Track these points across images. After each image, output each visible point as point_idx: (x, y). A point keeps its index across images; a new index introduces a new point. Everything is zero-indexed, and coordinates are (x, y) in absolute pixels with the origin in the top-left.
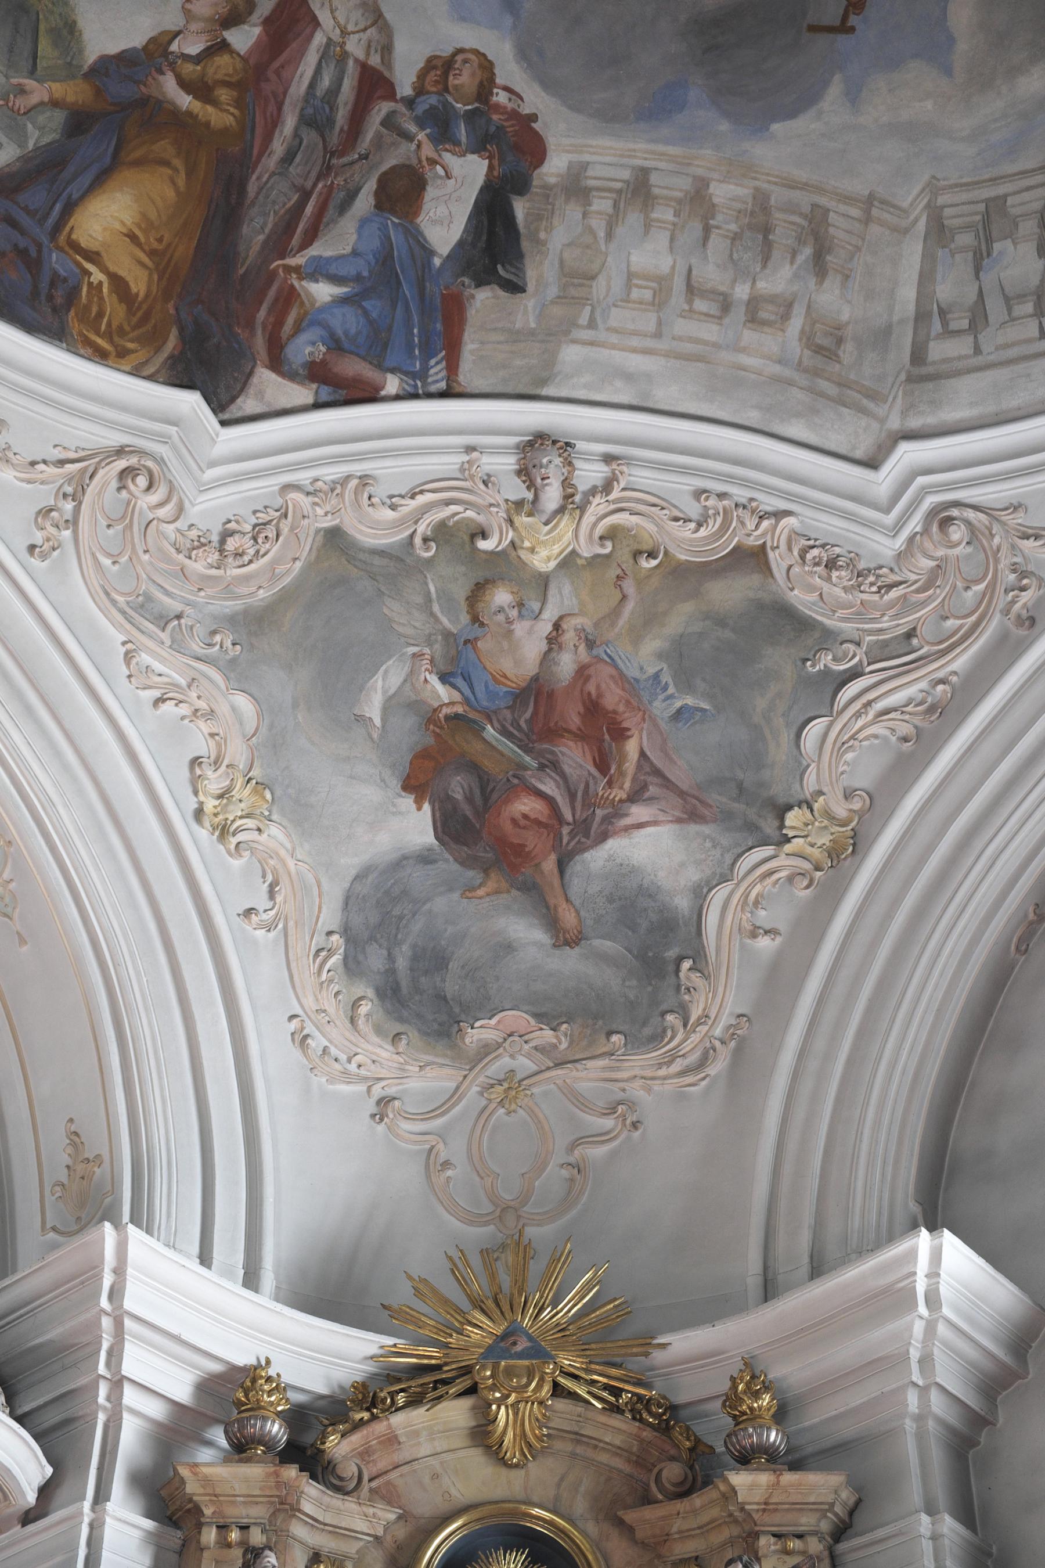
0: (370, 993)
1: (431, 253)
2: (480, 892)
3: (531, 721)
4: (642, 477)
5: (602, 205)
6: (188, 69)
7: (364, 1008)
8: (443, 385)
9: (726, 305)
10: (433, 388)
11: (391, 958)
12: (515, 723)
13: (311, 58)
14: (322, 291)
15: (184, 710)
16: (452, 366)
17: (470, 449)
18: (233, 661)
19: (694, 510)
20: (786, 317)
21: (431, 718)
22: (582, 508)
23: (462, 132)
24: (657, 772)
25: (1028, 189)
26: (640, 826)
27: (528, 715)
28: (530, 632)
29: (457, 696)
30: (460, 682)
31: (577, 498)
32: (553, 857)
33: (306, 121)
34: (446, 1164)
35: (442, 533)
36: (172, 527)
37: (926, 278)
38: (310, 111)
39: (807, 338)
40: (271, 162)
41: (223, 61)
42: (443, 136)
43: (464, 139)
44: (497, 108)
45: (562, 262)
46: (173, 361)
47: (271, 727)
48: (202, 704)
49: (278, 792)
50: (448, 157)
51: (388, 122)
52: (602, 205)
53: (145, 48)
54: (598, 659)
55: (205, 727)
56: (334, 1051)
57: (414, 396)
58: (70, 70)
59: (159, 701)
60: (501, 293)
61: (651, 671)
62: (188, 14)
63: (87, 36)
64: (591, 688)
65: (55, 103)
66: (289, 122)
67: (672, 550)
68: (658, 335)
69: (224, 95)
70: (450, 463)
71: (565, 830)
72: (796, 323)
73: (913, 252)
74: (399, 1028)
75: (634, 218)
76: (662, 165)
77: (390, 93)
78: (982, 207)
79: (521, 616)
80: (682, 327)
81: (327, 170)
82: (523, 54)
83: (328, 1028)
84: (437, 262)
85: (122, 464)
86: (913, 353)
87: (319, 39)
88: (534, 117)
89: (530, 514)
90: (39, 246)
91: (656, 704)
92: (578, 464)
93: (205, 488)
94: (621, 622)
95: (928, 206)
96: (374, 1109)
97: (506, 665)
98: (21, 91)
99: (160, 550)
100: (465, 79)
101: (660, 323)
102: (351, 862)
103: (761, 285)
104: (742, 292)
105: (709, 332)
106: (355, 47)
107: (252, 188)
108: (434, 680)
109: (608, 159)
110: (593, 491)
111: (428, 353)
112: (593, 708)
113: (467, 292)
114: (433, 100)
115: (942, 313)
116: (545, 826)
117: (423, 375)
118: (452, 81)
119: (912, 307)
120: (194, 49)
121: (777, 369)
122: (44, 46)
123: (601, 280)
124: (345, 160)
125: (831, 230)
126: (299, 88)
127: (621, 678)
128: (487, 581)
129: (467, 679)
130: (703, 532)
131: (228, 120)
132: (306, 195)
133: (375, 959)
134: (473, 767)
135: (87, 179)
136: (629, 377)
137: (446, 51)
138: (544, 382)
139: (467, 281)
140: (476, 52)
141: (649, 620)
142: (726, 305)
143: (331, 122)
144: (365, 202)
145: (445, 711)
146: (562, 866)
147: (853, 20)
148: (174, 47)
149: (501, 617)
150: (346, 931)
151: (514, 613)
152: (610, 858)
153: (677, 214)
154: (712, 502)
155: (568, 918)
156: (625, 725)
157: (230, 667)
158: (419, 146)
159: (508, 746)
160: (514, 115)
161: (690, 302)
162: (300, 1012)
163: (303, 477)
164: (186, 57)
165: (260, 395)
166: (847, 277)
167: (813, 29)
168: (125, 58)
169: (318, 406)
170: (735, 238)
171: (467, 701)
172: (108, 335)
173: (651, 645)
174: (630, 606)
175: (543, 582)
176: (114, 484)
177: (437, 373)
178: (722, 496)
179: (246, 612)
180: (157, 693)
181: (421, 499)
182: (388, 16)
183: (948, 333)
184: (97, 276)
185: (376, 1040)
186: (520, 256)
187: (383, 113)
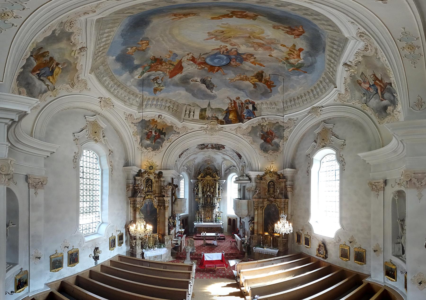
4: (270, 119)
14: (245, 114)
35: (259, 125)
41: (232, 107)
46: (239, 121)
51: (244, 105)
52: (260, 104)
57: (254, 118)
58: (224, 111)
66: (238, 107)
72: (276, 109)
73: (282, 104)
75: (263, 105)
77: (243, 103)
80: (269, 110)
81: (242, 108)
93: (244, 127)
102: (260, 144)
104: (271, 107)
105: (270, 110)
111: (253, 115)
133: (262, 149)
134: (265, 137)
136: (266, 113)
141: (272, 127)
142: (271, 108)
144: (245, 109)
163: (249, 124)
169: (248, 120)
175: (266, 126)
183: (286, 108)
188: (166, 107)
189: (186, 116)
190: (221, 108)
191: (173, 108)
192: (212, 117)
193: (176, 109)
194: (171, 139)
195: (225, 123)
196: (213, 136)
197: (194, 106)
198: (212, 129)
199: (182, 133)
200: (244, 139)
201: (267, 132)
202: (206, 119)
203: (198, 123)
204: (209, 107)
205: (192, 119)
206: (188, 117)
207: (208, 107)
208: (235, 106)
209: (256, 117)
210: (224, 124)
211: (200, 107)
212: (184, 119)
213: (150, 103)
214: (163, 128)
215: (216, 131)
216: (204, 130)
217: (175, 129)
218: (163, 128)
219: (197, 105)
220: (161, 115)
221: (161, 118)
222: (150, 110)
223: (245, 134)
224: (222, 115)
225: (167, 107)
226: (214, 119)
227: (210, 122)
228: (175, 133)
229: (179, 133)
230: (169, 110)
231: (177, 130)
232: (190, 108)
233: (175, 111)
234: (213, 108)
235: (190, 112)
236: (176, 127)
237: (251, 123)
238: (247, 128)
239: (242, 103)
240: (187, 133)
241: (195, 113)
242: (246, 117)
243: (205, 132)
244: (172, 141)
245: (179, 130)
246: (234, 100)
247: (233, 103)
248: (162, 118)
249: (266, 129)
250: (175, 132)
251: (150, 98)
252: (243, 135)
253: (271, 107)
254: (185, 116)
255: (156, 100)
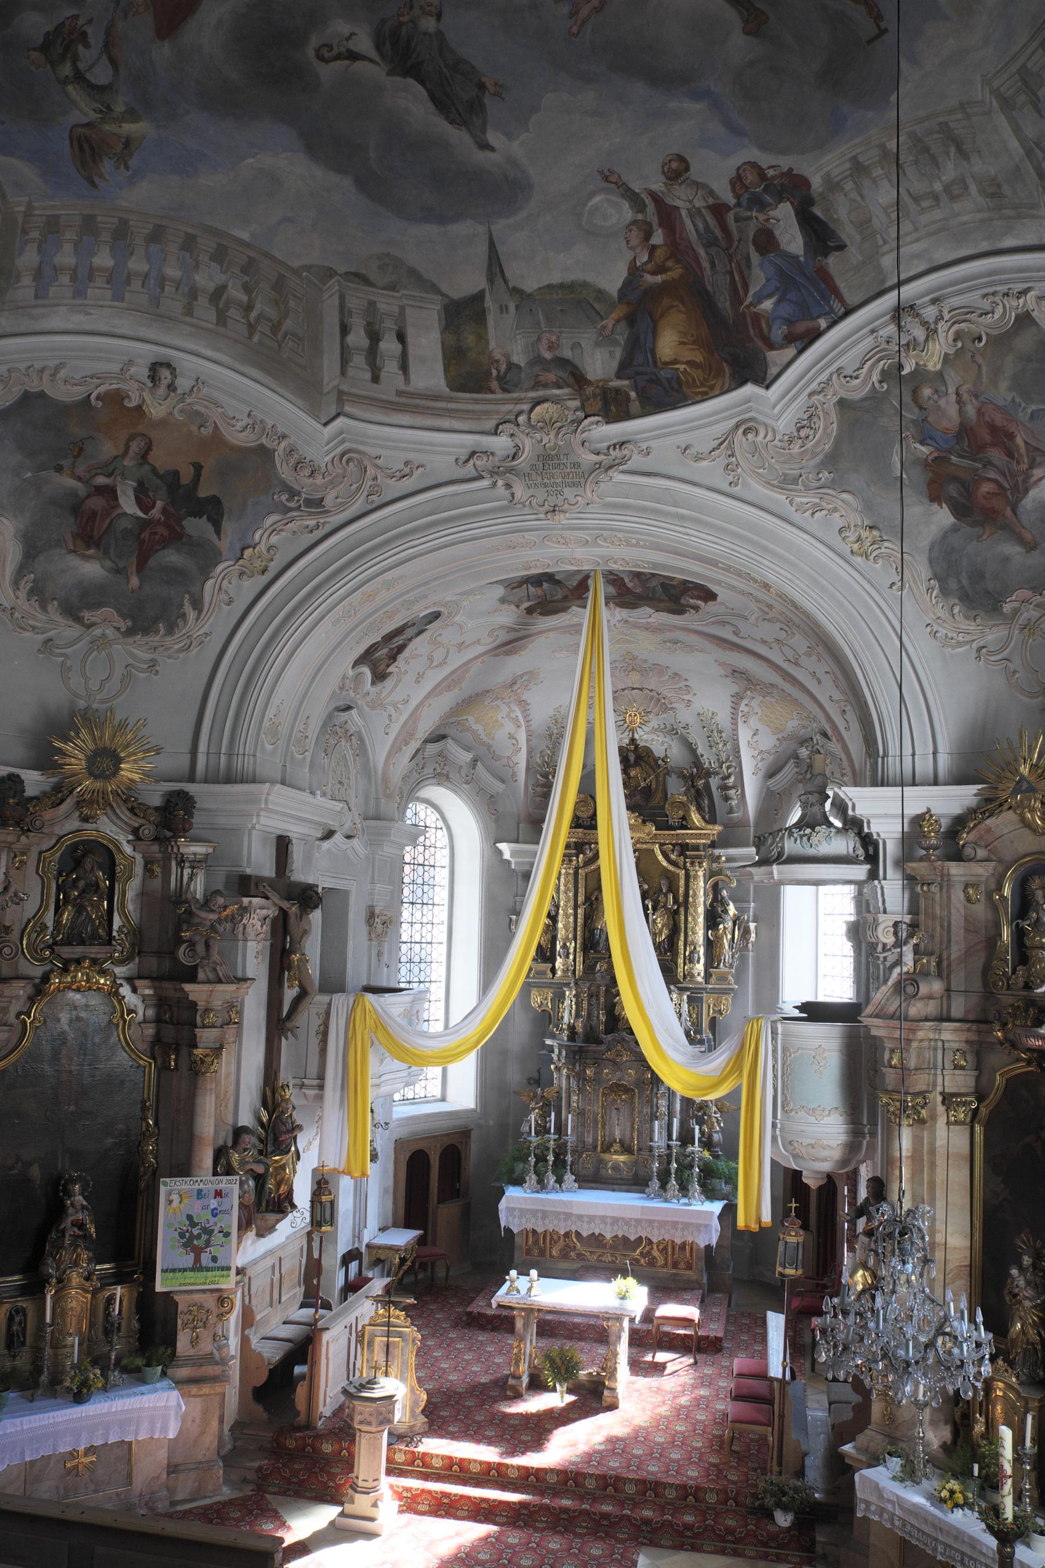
0: (956, 601)
1: (797, 257)
2: (985, 537)
3: (969, 446)
4: (956, 301)
5: (849, 186)
6: (650, 266)
7: (956, 610)
8: (843, 310)
9: (936, 198)
10: (840, 313)
11: (959, 582)
12: (963, 450)
13: (688, 222)
14: (767, 305)
15: (824, 512)
16: (842, 300)
17: (873, 331)
18: (833, 480)
19: (986, 305)
20: (966, 188)
21: (926, 464)
22: (936, 331)
23: (768, 198)
24: (1037, 449)
25: (1033, 53)
26: (1041, 479)
27: (966, 443)
28: (947, 402)
29: (931, 449)
30: (929, 441)
31: (932, 326)
32: (1009, 508)
33: (707, 246)
34: (1015, 672)
35: (885, 376)
36: (776, 441)
37: (1017, 130)
38: (705, 241)
39: (982, 192)
40: (708, 272)
41: (659, 252)
42: (763, 206)
43: (771, 201)
44: (773, 178)
45: (852, 222)
46: (733, 375)
47: (863, 500)
48: (830, 506)
49: (881, 526)
50: (771, 213)
51: (737, 220)
52: (849, 186)
53: (629, 274)
54: (983, 403)
55: (837, 515)
56: (950, 635)
59: (813, 514)
60: (837, 253)
61: (1009, 399)
62: (632, 248)
63: (607, 289)
64: (987, 418)
65: (618, 321)
66: (702, 252)
67: (990, 331)
68: (917, 230)
69: (670, 264)
70: (869, 342)
71: (1009, 493)
72: (973, 188)
73: (1001, 120)
74: (975, 613)
76: (859, 150)
77: (728, 208)
78: (1017, 77)
79: (940, 397)
80: (924, 219)
81: (730, 257)
82: (763, 148)
83: (944, 625)
84: (802, 259)
85: (741, 431)
86: (1037, 174)
87: (684, 213)
88: (791, 170)
89: (914, 349)
90: (654, 373)
91: (1020, 415)
92: (921, 312)
94: (984, 380)
95: (991, 92)
96: (975, 655)
97: (945, 424)
98: (604, 328)
99: (777, 453)
100: (750, 177)
101: (913, 223)
103: (944, 178)
104: (938, 187)
105: (937, 214)
106: (699, 203)
107: (709, 288)
108: (918, 446)
109: (834, 164)
110: (936, 322)
112: (993, 428)
113: (824, 263)
114: (746, 196)
115: (1037, 145)
116: (999, 494)
117: (832, 310)
118: (747, 182)
119: (1021, 151)
120: (645, 258)
121: (979, 216)
122: (597, 306)
123: (874, 219)
124: (734, 247)
125: (956, 132)
126: (693, 236)
127: (997, 408)
128: (916, 388)
129: (931, 438)
130: (997, 316)
131: (680, 271)
132: (731, 273)
133: (953, 584)
134: (956, 479)
135: (650, 336)
137: (733, 174)
138: (883, 281)
139: (820, 258)
140: (745, 163)
142: (936, 198)
143: (716, 238)
144: (755, 257)
145: (930, 458)
146: (1014, 511)
147: (883, 25)
148: (638, 264)
149: (931, 402)
150: (936, 576)
151: (936, 397)
152: (1034, 500)
153: (883, 168)
154: (991, 299)
155: (1028, 536)
156: (1011, 431)
157: (832, 485)
158: (757, 218)
159: (965, 462)
160: (782, 175)
161: (919, 205)
162: (929, 622)
163: (814, 386)
164: (645, 263)
165: (775, 364)
166: (979, 152)
167: (870, 41)
168: (627, 284)
169: (801, 352)
170: (916, 162)
171: (937, 449)
172: (702, 385)
173: (1004, 385)
174: (984, 369)
175: (940, 375)
176: (744, 439)
177: (836, 305)
178: (994, 294)
179: (826, 457)
180: (811, 511)
181: (866, 366)
182: (700, 180)
184: (682, 367)
185: (967, 622)
186: (833, 232)
187: (732, 218)
188: (193, 294)
189: (351, 372)
190: (585, 285)
191: (248, 308)
192: (537, 369)
193: (272, 313)
194: (263, 547)
195: (635, 406)
196: (562, 519)
197: (392, 287)
198: (546, 460)
199: (342, 507)
200: (796, 517)
201: (964, 431)
202: (494, 384)
203: (446, 423)
204: (499, 281)
205: (400, 393)
206: (368, 376)
207: (491, 280)
208: (677, 246)
209: (848, 313)
210: (627, 416)
211: (435, 289)
212: (341, 393)
213: (66, 257)
214: (198, 468)
215: (581, 476)
216: (493, 473)
217: (284, 471)
218: (198, 468)
219: (413, 273)
220: (168, 365)
221: (172, 387)
222: (77, 320)
223: (795, 480)
224: (605, 339)
225: (203, 301)
226: (551, 377)
227: (526, 407)
228: (292, 505)
229: (316, 504)
230: (222, 319)
231: (305, 484)
232: (372, 304)
233: (264, 328)
234: (530, 285)
235: (374, 337)
236: (292, 461)
237: (823, 377)
238: (805, 424)
239: (719, 210)
240: (377, 500)
241: (410, 339)
242: (778, 333)
243: (501, 490)
244: (274, 567)
245: (319, 480)
246: (653, 195)
247: (655, 220)
248: (183, 383)
249: (952, 410)
250: (293, 493)
251: (57, 217)
252: (787, 483)
253: (938, 187)
254: (343, 373)
255: (105, 236)
